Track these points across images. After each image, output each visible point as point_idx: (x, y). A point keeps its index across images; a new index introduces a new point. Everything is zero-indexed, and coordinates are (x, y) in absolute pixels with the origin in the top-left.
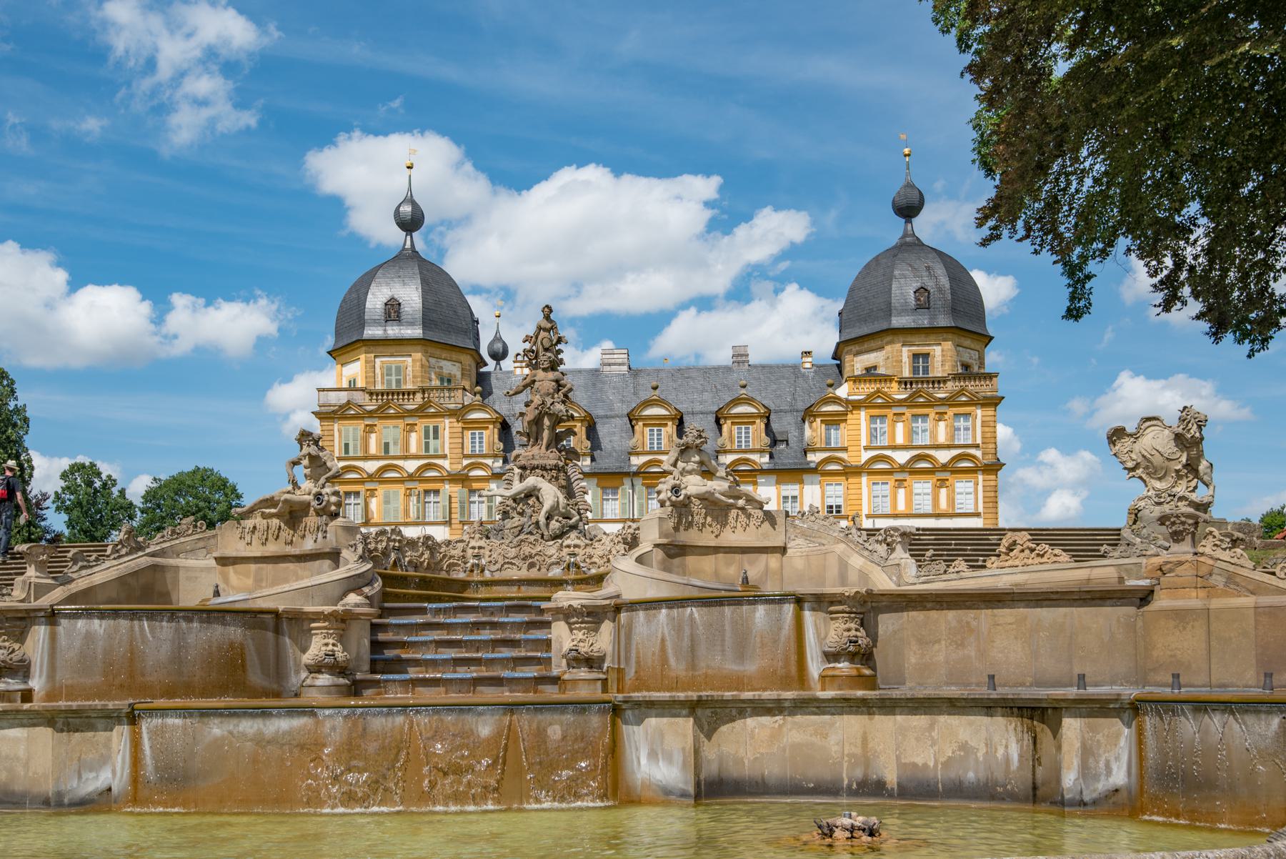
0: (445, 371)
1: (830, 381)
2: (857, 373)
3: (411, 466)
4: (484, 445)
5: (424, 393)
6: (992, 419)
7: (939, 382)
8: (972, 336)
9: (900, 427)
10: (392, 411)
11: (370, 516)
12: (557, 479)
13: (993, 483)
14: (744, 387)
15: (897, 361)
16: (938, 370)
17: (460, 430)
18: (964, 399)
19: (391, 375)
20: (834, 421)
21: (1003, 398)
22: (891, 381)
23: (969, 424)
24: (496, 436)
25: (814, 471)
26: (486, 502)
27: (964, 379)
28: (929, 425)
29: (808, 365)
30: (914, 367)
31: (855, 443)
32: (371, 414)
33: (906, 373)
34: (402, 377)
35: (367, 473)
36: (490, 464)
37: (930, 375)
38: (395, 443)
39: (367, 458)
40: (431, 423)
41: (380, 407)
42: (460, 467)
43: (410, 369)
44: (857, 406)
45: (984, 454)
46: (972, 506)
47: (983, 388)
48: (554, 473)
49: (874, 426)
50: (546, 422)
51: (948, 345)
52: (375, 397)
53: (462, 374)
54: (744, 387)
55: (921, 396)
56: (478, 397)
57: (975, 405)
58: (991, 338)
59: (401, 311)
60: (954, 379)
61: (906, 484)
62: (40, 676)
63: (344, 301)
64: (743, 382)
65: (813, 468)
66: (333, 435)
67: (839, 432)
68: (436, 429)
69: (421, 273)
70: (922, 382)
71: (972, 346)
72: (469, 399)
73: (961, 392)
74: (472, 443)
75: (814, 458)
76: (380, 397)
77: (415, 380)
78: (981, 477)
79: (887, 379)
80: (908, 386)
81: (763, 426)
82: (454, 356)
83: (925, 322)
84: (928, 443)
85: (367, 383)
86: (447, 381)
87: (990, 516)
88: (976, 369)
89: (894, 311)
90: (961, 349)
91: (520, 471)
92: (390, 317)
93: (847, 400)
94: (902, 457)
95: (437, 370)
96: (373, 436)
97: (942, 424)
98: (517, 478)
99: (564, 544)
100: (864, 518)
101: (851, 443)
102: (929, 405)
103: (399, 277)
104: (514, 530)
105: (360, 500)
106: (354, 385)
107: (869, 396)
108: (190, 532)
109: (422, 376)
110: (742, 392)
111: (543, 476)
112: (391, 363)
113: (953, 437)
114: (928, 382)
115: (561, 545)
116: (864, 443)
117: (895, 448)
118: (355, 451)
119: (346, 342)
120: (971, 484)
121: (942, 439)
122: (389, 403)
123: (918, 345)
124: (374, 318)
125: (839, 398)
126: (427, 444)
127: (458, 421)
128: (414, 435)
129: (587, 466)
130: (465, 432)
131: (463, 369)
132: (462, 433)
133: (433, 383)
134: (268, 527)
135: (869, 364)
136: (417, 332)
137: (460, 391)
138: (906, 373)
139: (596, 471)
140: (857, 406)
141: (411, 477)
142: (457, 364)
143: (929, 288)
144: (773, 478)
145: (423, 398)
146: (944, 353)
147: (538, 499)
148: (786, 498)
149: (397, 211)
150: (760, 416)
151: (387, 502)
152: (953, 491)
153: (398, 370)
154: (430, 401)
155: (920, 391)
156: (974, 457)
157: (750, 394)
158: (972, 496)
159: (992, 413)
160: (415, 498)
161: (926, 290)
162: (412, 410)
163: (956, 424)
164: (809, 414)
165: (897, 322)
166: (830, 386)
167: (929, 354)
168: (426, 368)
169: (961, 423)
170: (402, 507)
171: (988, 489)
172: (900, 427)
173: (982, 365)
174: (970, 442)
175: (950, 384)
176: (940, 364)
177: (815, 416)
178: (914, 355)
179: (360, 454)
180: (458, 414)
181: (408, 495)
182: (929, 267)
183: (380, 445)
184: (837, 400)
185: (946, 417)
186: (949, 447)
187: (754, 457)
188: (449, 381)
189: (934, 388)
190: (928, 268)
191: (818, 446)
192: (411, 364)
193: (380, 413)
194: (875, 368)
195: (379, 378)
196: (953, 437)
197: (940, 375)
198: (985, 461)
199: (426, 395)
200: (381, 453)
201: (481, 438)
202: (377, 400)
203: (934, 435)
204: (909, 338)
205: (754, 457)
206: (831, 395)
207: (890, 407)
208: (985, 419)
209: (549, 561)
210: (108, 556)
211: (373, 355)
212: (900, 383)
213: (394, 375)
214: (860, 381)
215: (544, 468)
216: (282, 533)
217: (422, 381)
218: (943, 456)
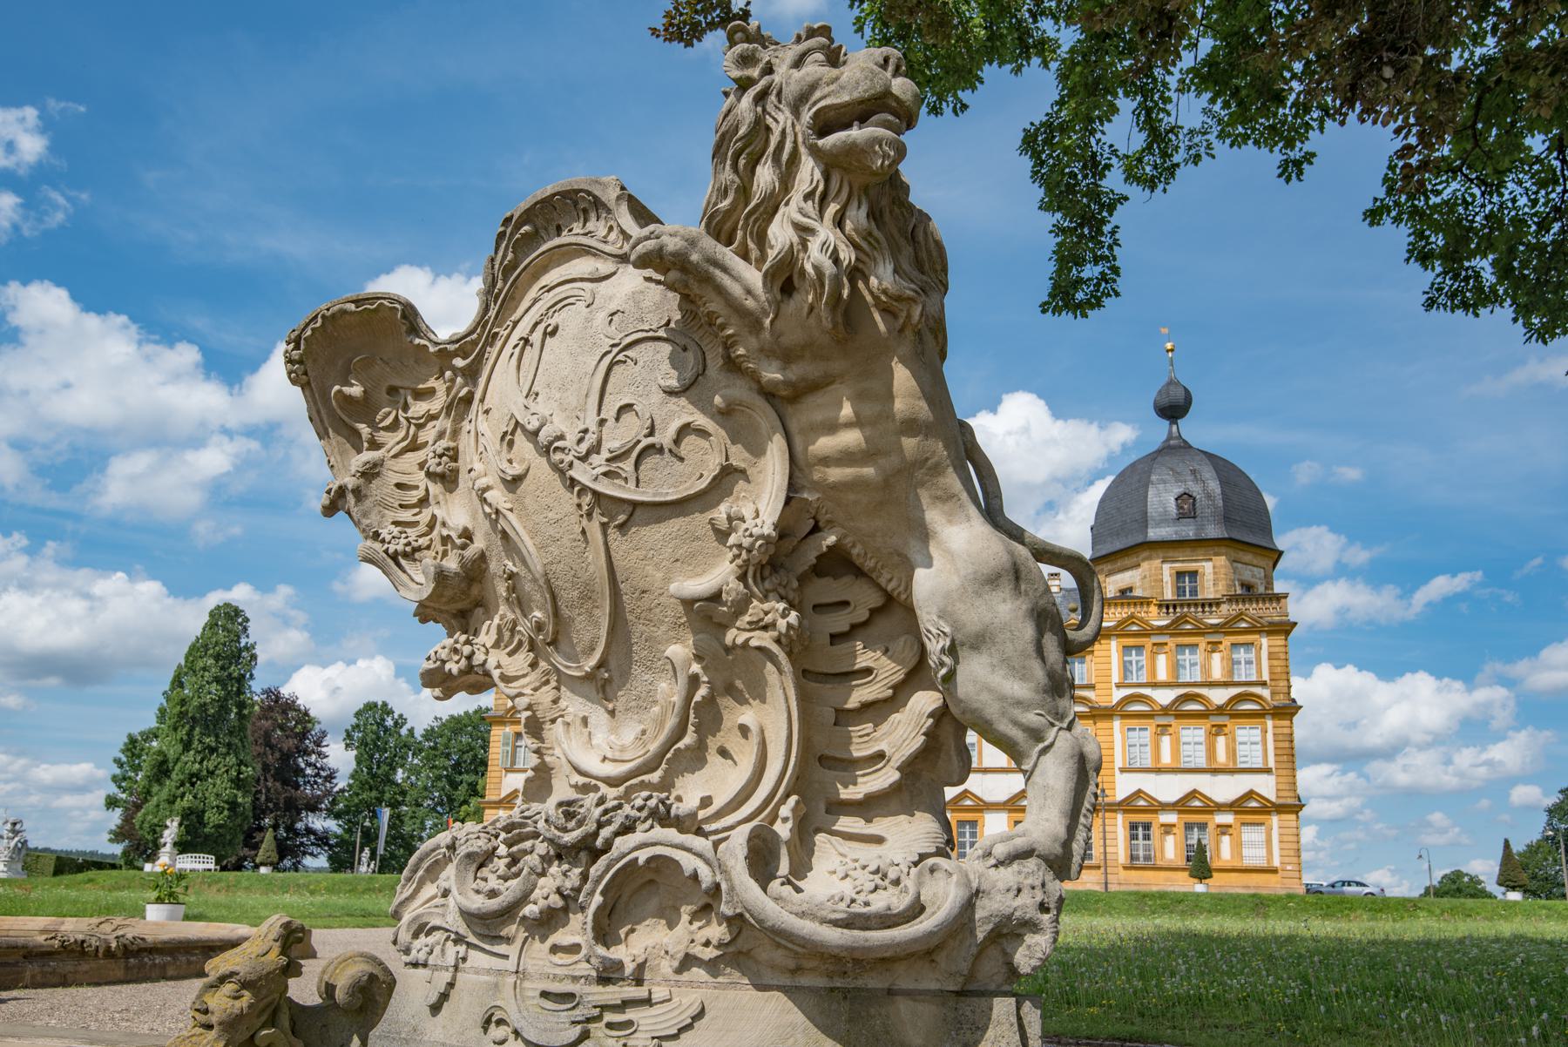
6: (1283, 649)
7: (1210, 605)
8: (1254, 550)
9: (1162, 661)
15: (1156, 581)
18: (1244, 625)
21: (1295, 624)
22: (1149, 604)
23: (1252, 656)
27: (1244, 602)
28: (1199, 657)
30: (1178, 588)
31: (1104, 679)
33: (1169, 594)
47: (1269, 612)
49: (1126, 658)
51: (1221, 560)
57: (1259, 632)
58: (1281, 553)
67: (1085, 665)
71: (1255, 562)
73: (1239, 617)
79: (1144, 602)
80: (1171, 610)
83: (1188, 531)
84: (1199, 679)
88: (1261, 590)
90: (1239, 565)
94: (1164, 697)
97: (1216, 657)
101: (1100, 679)
107: (1121, 623)
113: (1231, 672)
114: (1196, 605)
116: (1116, 678)
117: (1155, 685)
121: (1217, 674)
123: (1183, 561)
135: (1123, 585)
138: (1169, 594)
159: (1283, 643)
163: (1235, 656)
169: (1241, 655)
172: (1162, 661)
173: (1269, 583)
174: (1254, 678)
175: (1224, 608)
185: (1221, 647)
186: (1226, 685)
194: (1131, 589)
196: (1231, 672)
197: (1212, 596)
203: (1206, 669)
204: (1171, 553)
207: (1148, 635)
208: (1273, 650)
212: (1160, 606)
218: (1219, 696)
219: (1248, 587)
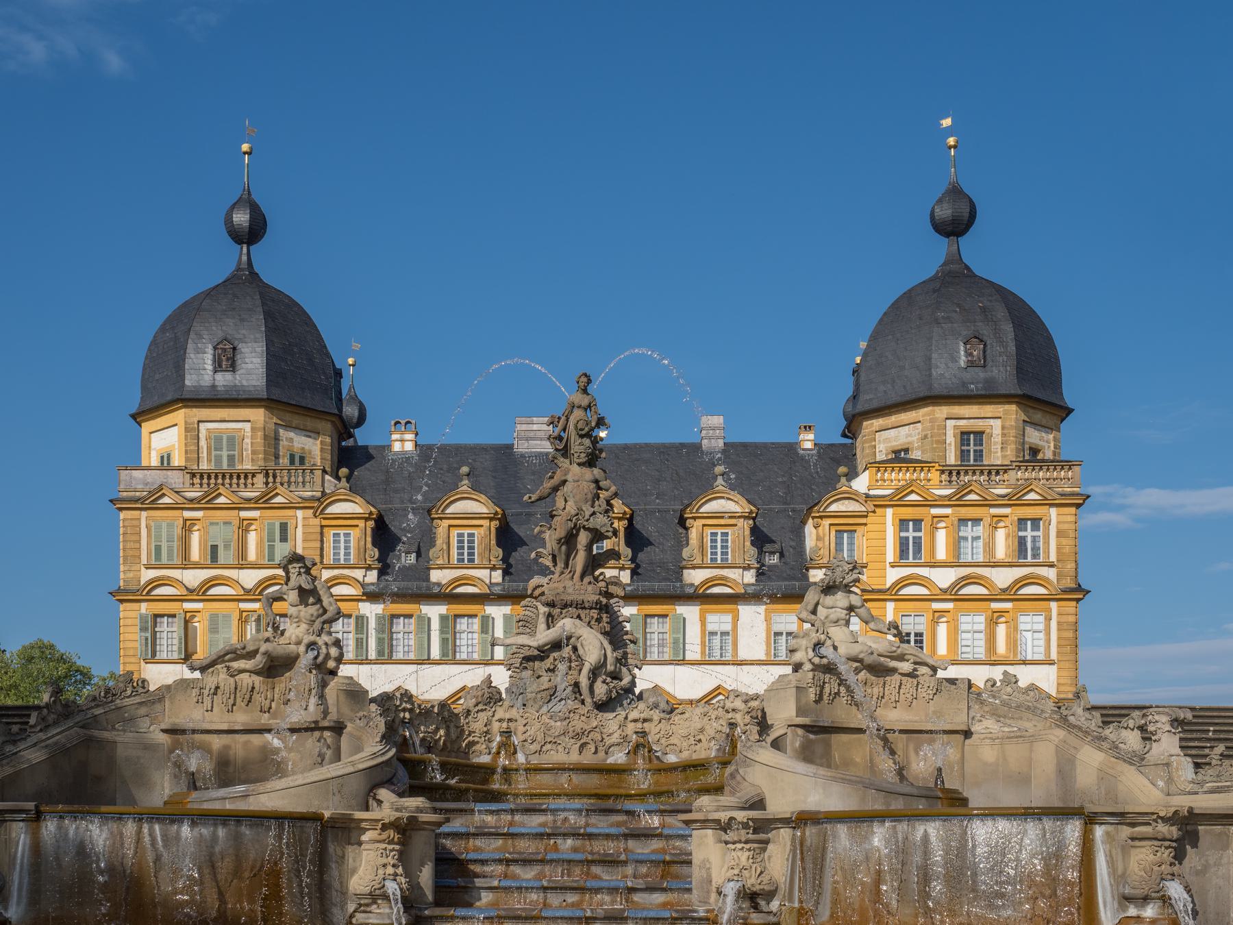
2: (880, 457)
4: (352, 551)
12: (599, 620)
15: (938, 442)
16: (996, 454)
19: (221, 449)
24: (369, 539)
29: (809, 445)
30: (962, 451)
33: (952, 458)
34: (236, 453)
37: (985, 463)
38: (227, 547)
39: (187, 564)
41: (206, 495)
43: (248, 441)
46: (1042, 650)
48: (594, 613)
50: (583, 538)
56: (344, 482)
62: (18, 903)
63: (154, 343)
68: (284, 527)
69: (263, 304)
71: (1044, 422)
77: (255, 457)
80: (954, 478)
84: (980, 558)
85: (187, 460)
88: (1049, 455)
91: (546, 609)
92: (220, 366)
93: (867, 496)
98: (542, 619)
99: (631, 717)
102: (985, 503)
104: (544, 694)
106: (169, 463)
108: (129, 692)
109: (265, 452)
111: (579, 617)
115: (626, 718)
118: (170, 557)
119: (156, 401)
120: (1041, 619)
122: (219, 489)
125: (856, 493)
126: (271, 548)
128: (252, 538)
130: (326, 530)
132: (322, 534)
134: (236, 688)
141: (249, 595)
143: (985, 338)
145: (267, 483)
146: (1005, 431)
147: (575, 649)
152: (1016, 629)
153: (232, 441)
156: (1046, 579)
158: (1041, 635)
160: (254, 624)
161: (982, 341)
172: (941, 536)
176: (999, 447)
178: (962, 433)
183: (205, 545)
186: (1011, 565)
188: (302, 459)
192: (249, 434)
193: (207, 502)
195: (204, 454)
199: (271, 479)
200: (205, 559)
203: (990, 547)
205: (733, 574)
209: (608, 741)
210: (32, 727)
212: (943, 472)
215: (580, 606)
216: (256, 697)
218: (1003, 578)
219: (1035, 451)
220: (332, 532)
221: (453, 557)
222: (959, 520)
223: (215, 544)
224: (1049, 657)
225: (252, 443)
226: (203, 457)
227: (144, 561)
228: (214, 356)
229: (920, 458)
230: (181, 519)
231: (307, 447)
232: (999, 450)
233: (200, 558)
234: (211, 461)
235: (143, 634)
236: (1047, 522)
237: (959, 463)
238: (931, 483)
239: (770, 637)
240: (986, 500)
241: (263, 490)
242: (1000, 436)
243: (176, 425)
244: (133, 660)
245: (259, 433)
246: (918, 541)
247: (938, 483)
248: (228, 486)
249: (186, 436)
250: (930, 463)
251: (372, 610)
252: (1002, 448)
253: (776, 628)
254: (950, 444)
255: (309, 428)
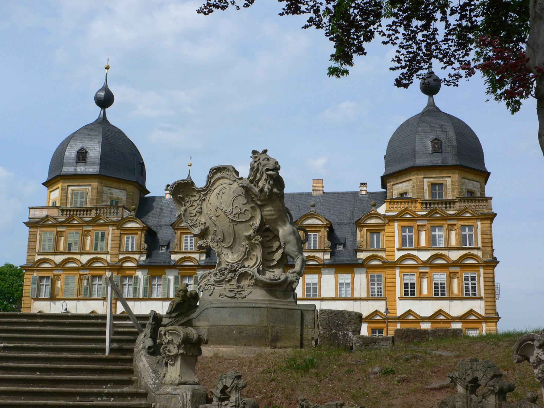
0: (115, 196)
1: (372, 203)
3: (84, 259)
4: (134, 245)
5: (97, 210)
7: (450, 203)
10: (76, 222)
11: (56, 293)
13: (491, 275)
14: (314, 206)
15: (420, 189)
17: (119, 235)
19: (77, 198)
20: (376, 230)
22: (416, 202)
24: (143, 239)
25: (362, 265)
26: (133, 285)
27: (468, 201)
32: (61, 224)
33: (427, 197)
34: (84, 200)
35: (55, 263)
36: (138, 259)
37: (444, 199)
38: (76, 244)
39: (56, 253)
40: (99, 230)
41: (67, 219)
42: (117, 260)
44: (391, 219)
45: (483, 254)
47: (482, 208)
49: (404, 234)
52: (65, 213)
53: (127, 198)
54: (314, 206)
55: (437, 213)
57: (477, 219)
59: (87, 156)
60: (460, 201)
61: (428, 275)
64: (312, 203)
65: (360, 264)
66: (36, 238)
68: (103, 234)
70: (438, 203)
71: (475, 179)
72: (126, 213)
73: (466, 210)
74: (127, 244)
75: (362, 256)
76: (68, 213)
77: (92, 201)
78: (482, 271)
79: (413, 201)
80: (428, 206)
81: (326, 234)
82: (122, 186)
84: (443, 246)
85: (61, 203)
86: (115, 204)
87: (490, 299)
88: (478, 195)
89: (417, 155)
90: (466, 181)
95: (109, 195)
96: (63, 238)
100: (398, 300)
103: (89, 135)
105: (49, 283)
106: (55, 205)
109: (97, 199)
110: (311, 210)
112: (78, 190)
114: (442, 203)
116: (397, 245)
118: (49, 249)
122: (74, 216)
123: (435, 177)
124: (69, 161)
125: (379, 214)
126: (96, 245)
127: (118, 229)
128: (89, 240)
129: (203, 260)
130: (122, 236)
131: (127, 195)
132: (120, 237)
133: (104, 204)
135: (402, 191)
136: (94, 169)
137: (121, 209)
138: (427, 197)
139: (208, 264)
140: (391, 219)
141: (84, 267)
142: (124, 191)
143: (441, 139)
144: (333, 270)
145: (96, 213)
148: (341, 284)
149: (96, 95)
150: (324, 227)
151: (67, 283)
154: (100, 216)
155: (436, 209)
157: (318, 211)
159: (489, 225)
162: (88, 222)
164: (359, 224)
165: (420, 162)
166: (374, 205)
167: (442, 184)
168: (100, 193)
170: (77, 288)
171: (488, 279)
172: (423, 235)
175: (457, 205)
176: (451, 190)
177: (362, 227)
178: (432, 184)
179: (52, 251)
180: (119, 224)
181: (81, 279)
182: (442, 125)
184: (378, 216)
185: (456, 228)
186: (458, 249)
187: (319, 255)
188: (117, 203)
189: (446, 208)
190: (441, 126)
191: (365, 247)
193: (67, 223)
194: (406, 193)
195: (69, 201)
197: (451, 198)
198: (485, 260)
199: (98, 212)
201: (133, 241)
202: (66, 215)
203: (448, 240)
205: (319, 255)
206: (373, 212)
211: (66, 185)
212: (422, 203)
213: (79, 199)
214: (394, 202)
217: (97, 202)
218: (454, 256)
220: (126, 236)
221: (183, 247)
222: (431, 226)
223: (70, 242)
224: (480, 295)
225: (91, 195)
226: (69, 202)
227: (37, 251)
228: (77, 156)
229: (412, 197)
230: (56, 231)
231: (120, 197)
232: (451, 192)
233: (63, 249)
234: (72, 204)
235: (33, 286)
236: (476, 227)
237: (431, 199)
238: (417, 208)
239: (337, 286)
240: (444, 217)
241: (94, 217)
242: (451, 186)
243: (58, 188)
244: (28, 298)
245: (95, 191)
246: (411, 238)
247: (420, 209)
248: (78, 215)
249: (62, 192)
250: (416, 199)
251: (140, 274)
252: (452, 191)
253: (341, 281)
254: (426, 190)
255: (122, 188)
